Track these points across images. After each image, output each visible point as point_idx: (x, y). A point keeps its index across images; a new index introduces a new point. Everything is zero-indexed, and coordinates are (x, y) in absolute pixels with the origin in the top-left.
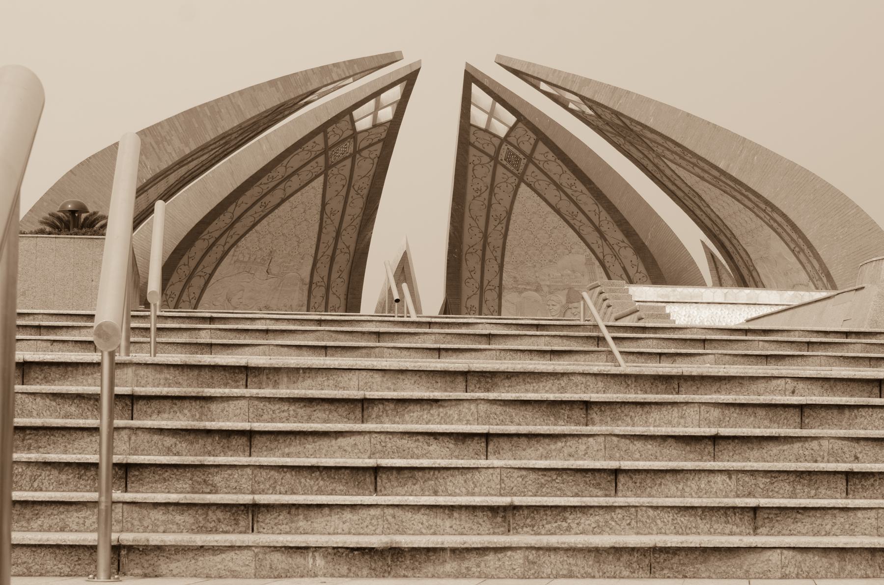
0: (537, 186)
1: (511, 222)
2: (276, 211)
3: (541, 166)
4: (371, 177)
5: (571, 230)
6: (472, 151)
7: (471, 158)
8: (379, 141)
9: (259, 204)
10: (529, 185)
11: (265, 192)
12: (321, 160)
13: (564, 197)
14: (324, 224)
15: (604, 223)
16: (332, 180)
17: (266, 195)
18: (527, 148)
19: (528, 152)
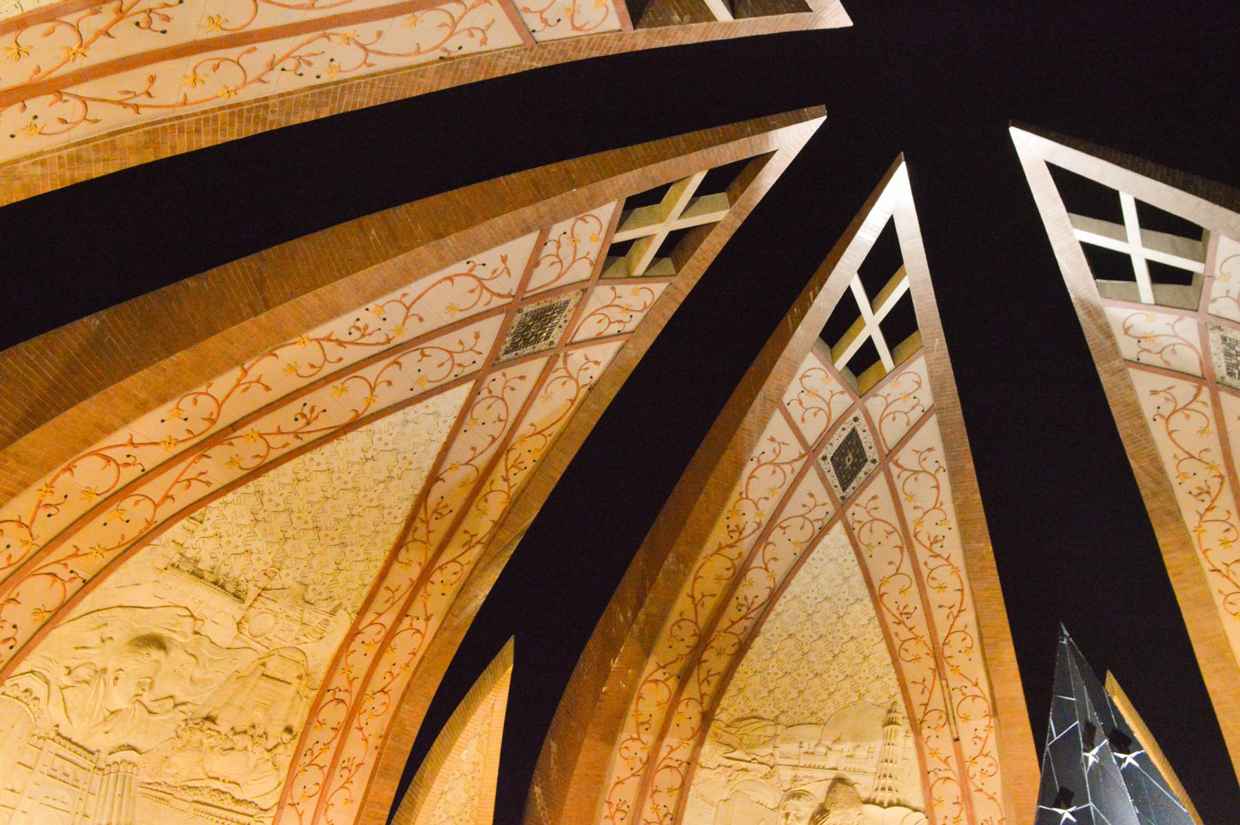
0: (865, 537)
1: (772, 616)
2: (327, 448)
3: (898, 484)
4: (549, 439)
5: (883, 646)
7: (763, 446)
9: (295, 407)
10: (849, 530)
11: (329, 369)
12: (490, 328)
13: (907, 567)
14: (410, 538)
16: (479, 410)
17: (327, 380)
18: (892, 432)
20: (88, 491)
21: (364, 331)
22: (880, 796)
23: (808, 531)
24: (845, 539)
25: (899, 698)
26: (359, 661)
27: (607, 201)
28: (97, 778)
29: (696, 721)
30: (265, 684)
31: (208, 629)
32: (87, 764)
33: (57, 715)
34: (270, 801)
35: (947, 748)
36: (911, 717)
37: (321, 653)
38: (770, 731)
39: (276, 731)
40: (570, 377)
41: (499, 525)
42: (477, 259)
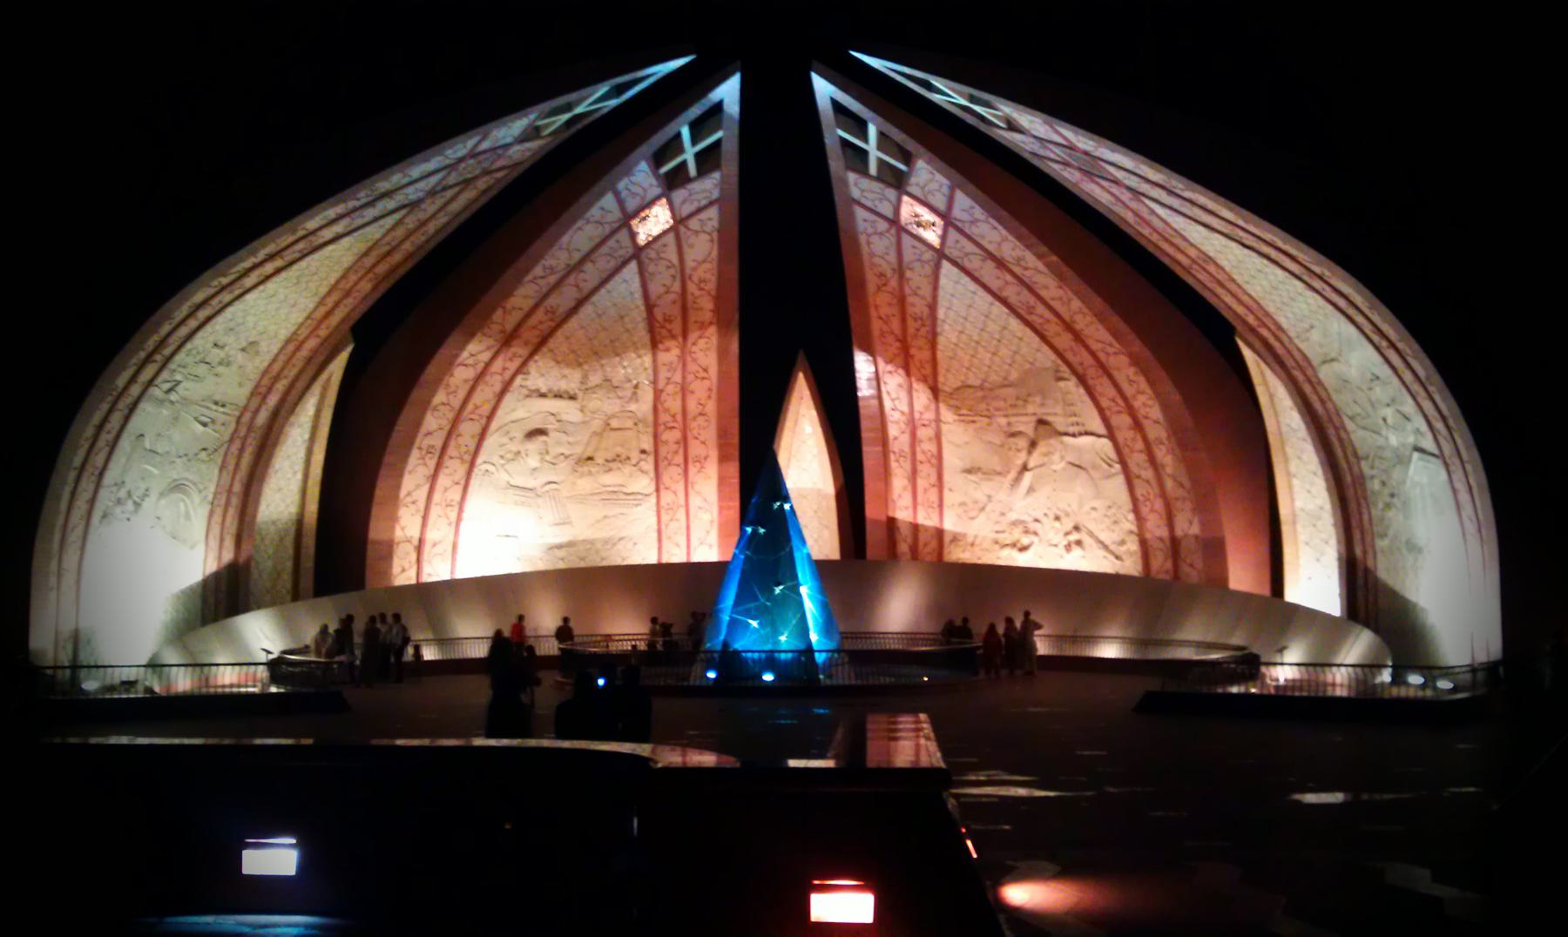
0: (968, 265)
4: (715, 263)
6: (860, 214)
8: (711, 204)
11: (544, 290)
15: (1078, 318)
16: (651, 268)
19: (942, 206)
20: (466, 381)
21: (551, 268)
22: (1071, 430)
23: (928, 269)
24: (955, 270)
25: (1059, 362)
26: (674, 404)
27: (637, 163)
28: (540, 501)
29: (928, 392)
30: (613, 434)
31: (564, 417)
32: (531, 494)
33: (504, 477)
34: (652, 488)
35: (1112, 392)
36: (1074, 372)
37: (644, 406)
38: (980, 394)
39: (635, 456)
40: (697, 232)
41: (717, 311)
42: (588, 215)
